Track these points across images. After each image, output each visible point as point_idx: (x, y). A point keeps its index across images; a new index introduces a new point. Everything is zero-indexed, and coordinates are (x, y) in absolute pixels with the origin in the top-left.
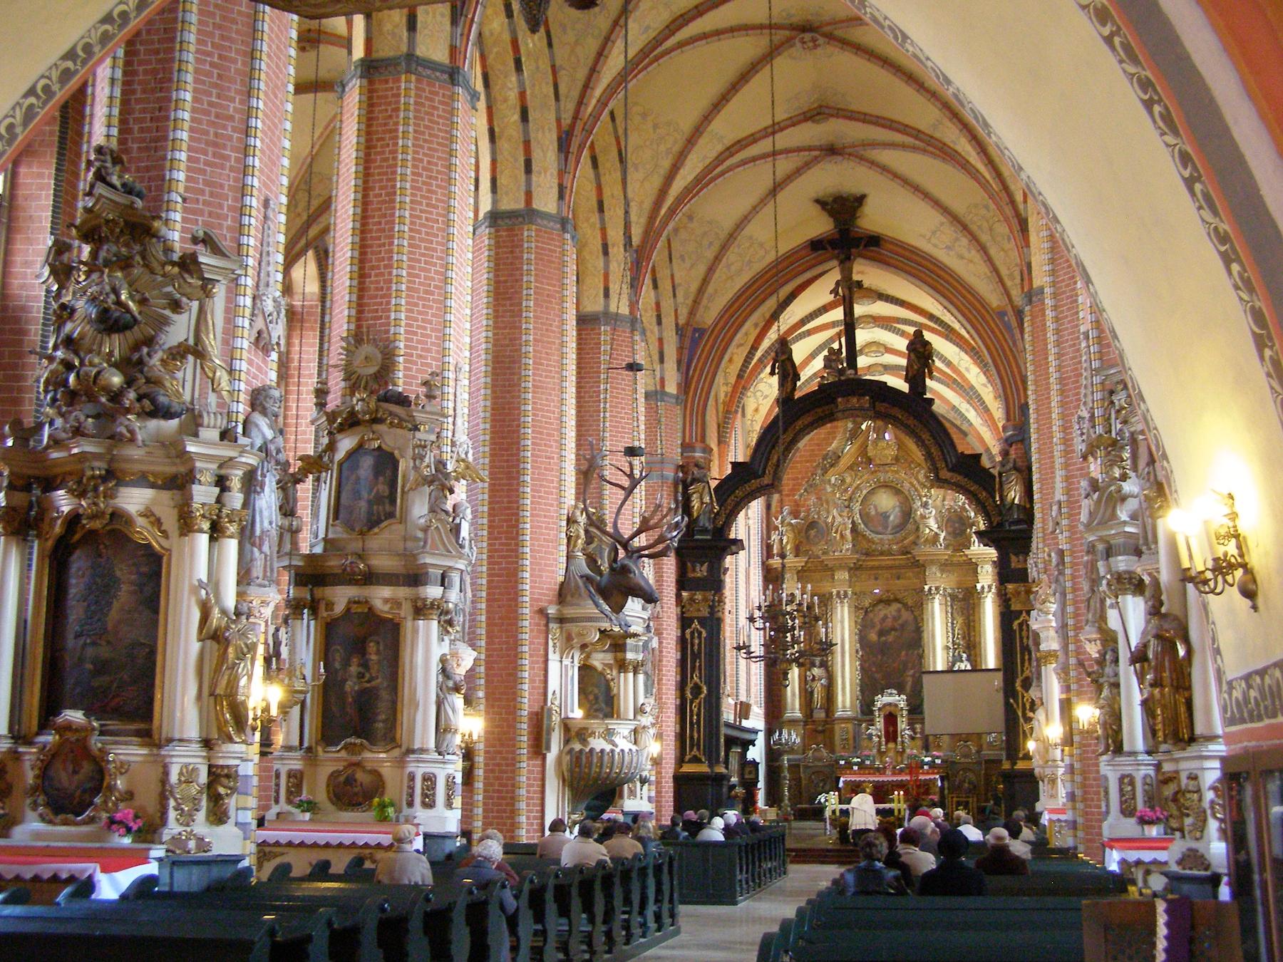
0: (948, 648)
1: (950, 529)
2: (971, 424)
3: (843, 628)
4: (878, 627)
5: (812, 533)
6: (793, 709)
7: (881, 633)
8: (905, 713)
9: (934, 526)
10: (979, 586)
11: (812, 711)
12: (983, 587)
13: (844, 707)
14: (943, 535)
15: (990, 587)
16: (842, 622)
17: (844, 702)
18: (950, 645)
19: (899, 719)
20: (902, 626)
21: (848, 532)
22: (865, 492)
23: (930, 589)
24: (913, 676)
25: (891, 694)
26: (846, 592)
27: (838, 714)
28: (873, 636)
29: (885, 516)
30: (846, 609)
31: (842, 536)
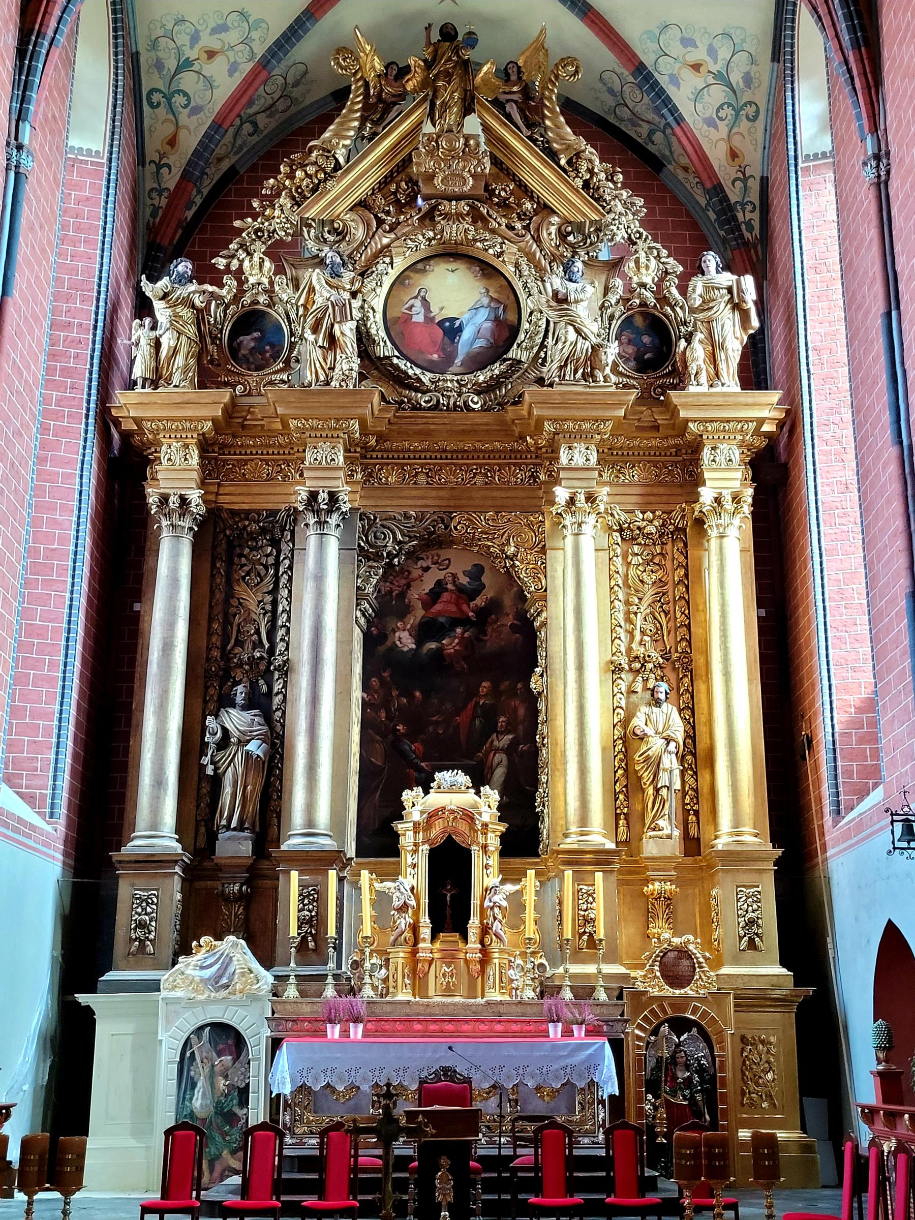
0: (617, 669)
1: (630, 349)
2: (679, 120)
3: (320, 594)
4: (419, 613)
5: (248, 341)
6: (155, 825)
7: (425, 631)
8: (494, 842)
9: (592, 327)
10: (706, 495)
11: (212, 837)
12: (718, 500)
13: (310, 822)
14: (612, 351)
15: (736, 499)
16: (319, 578)
17: (310, 807)
18: (624, 661)
19: (477, 860)
20: (484, 613)
21: (347, 331)
22: (400, 264)
23: (572, 501)
24: (509, 751)
25: (453, 789)
26: (333, 497)
27: (292, 843)
28: (405, 640)
29: (451, 329)
30: (333, 545)
31: (332, 340)
